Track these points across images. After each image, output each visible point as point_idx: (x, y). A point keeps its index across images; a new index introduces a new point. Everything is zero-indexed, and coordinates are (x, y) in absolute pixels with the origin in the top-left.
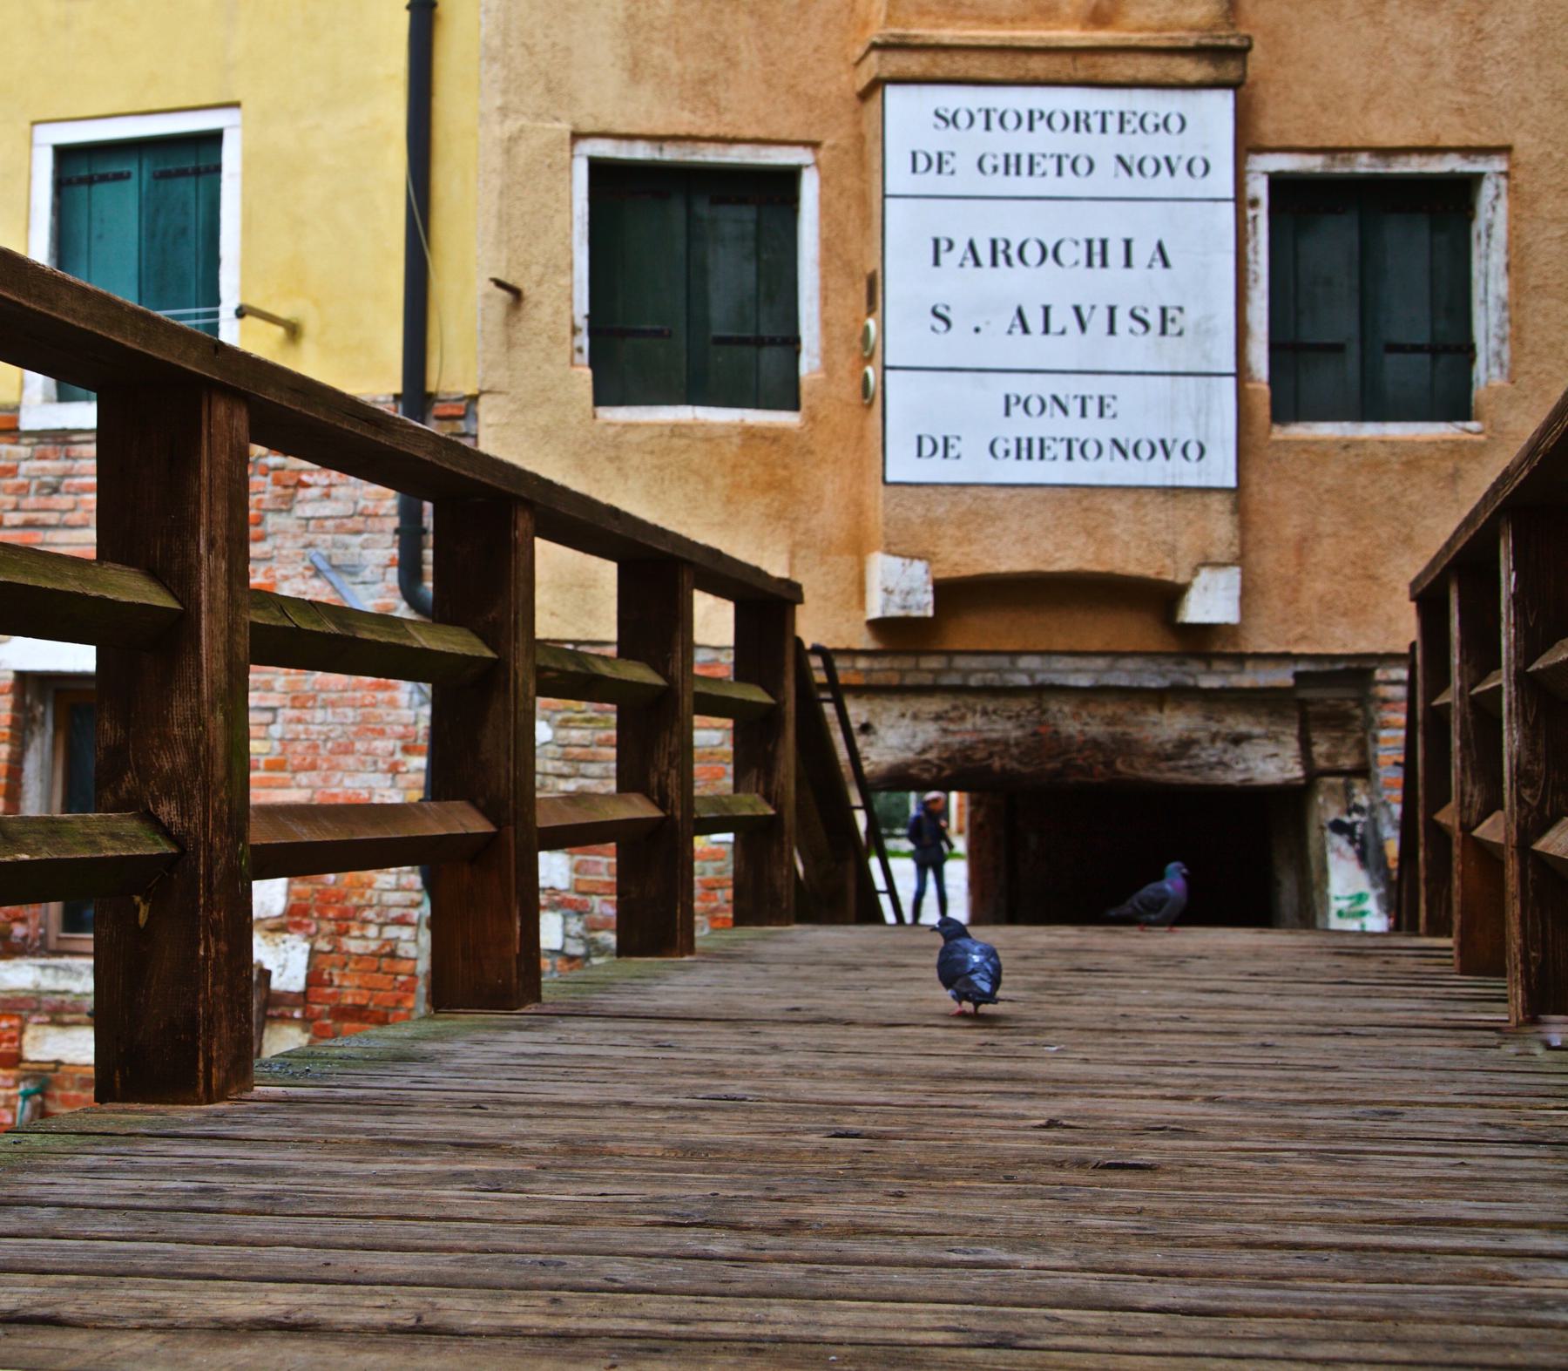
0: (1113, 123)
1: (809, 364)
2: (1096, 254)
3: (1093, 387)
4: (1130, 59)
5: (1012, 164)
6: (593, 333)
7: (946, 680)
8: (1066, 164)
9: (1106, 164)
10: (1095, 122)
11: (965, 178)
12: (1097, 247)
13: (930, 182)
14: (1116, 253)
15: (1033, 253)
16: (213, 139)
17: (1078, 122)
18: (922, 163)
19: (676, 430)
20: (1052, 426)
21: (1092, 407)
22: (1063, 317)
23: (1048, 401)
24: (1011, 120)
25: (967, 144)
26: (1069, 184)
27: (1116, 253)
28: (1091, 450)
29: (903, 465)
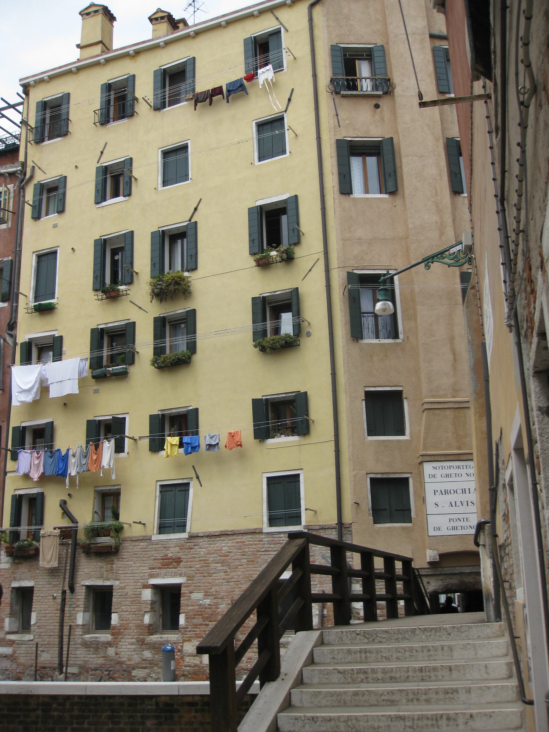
0: (465, 467)
1: (413, 514)
2: (464, 491)
3: (465, 516)
4: (467, 455)
5: (447, 476)
6: (373, 510)
7: (443, 572)
8: (457, 475)
9: (464, 475)
10: (461, 467)
11: (439, 479)
12: (464, 490)
13: (433, 480)
14: (467, 491)
15: (452, 492)
16: (298, 475)
17: (458, 467)
18: (431, 476)
19: (389, 528)
20: (458, 524)
21: (465, 520)
22: (458, 503)
23: (457, 519)
24: (446, 468)
25: (438, 472)
26: (458, 479)
27: (467, 491)
28: (466, 528)
29: (432, 533)
